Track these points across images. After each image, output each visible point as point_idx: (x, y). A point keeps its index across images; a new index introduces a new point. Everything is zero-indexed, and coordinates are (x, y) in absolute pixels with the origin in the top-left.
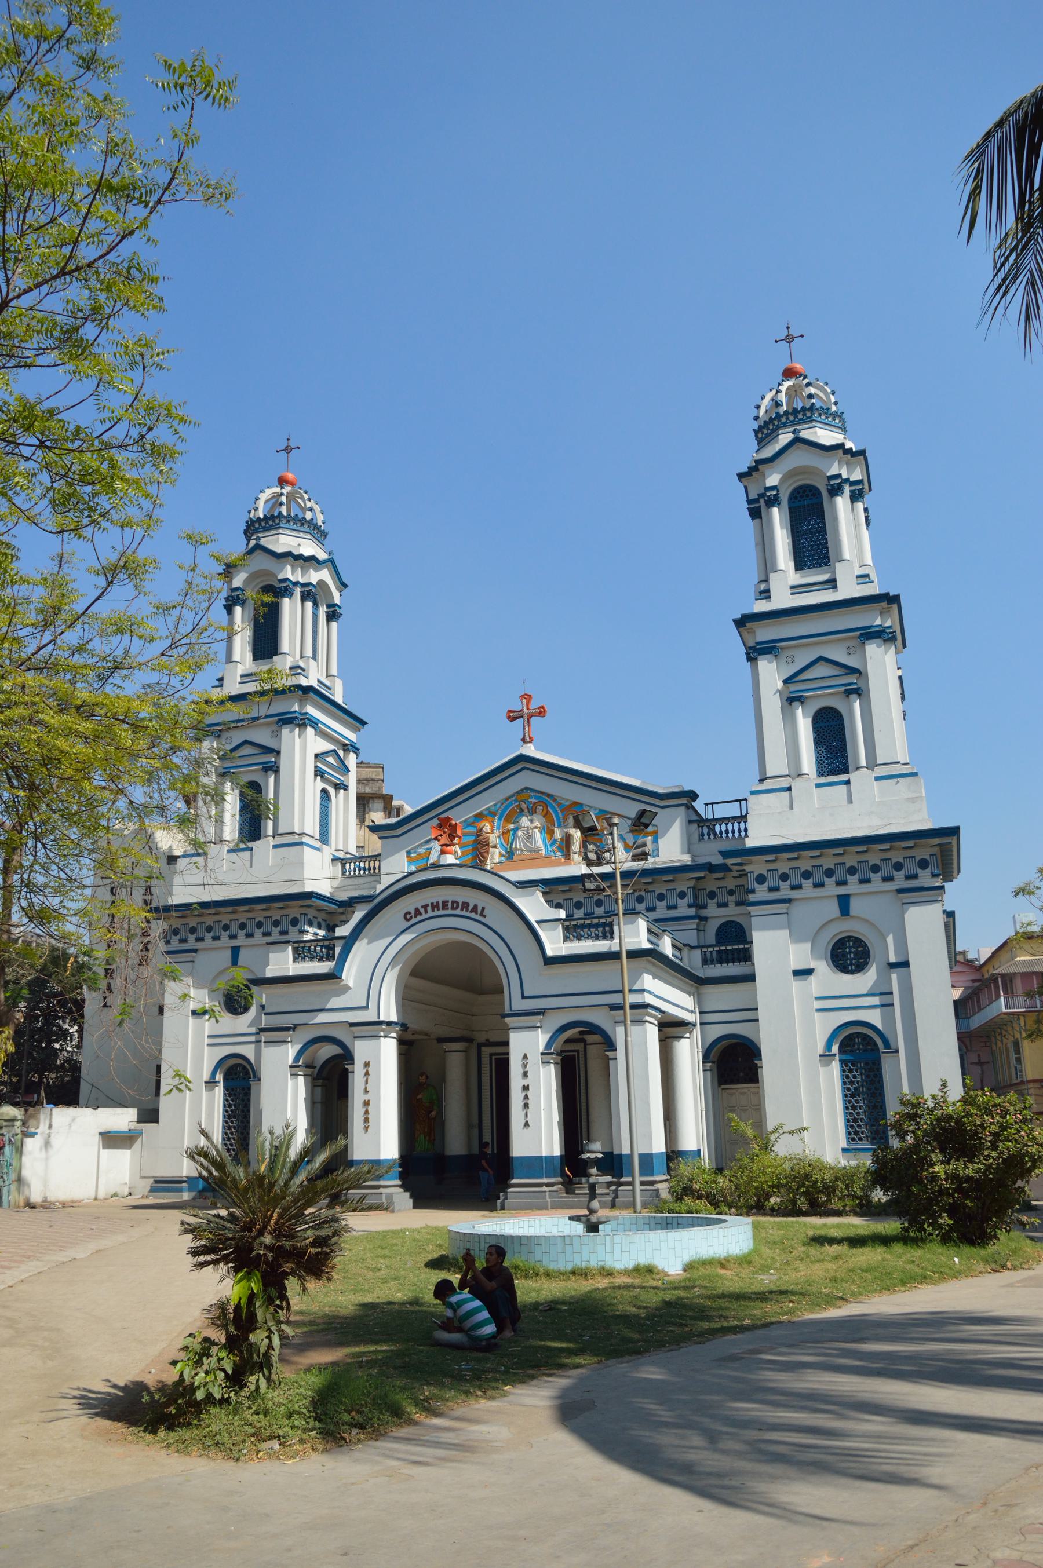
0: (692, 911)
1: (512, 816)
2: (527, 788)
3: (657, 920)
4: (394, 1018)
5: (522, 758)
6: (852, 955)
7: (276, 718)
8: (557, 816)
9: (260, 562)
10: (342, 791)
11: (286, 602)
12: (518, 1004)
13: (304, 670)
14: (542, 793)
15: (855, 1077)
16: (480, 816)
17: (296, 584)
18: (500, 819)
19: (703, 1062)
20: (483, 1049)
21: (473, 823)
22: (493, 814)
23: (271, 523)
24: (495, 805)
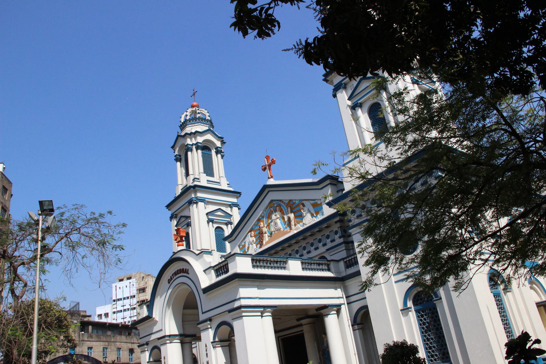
0: (342, 240)
1: (269, 217)
3: (327, 250)
4: (176, 332)
5: (265, 187)
7: (187, 204)
8: (284, 209)
9: (181, 142)
10: (229, 225)
11: (189, 153)
13: (198, 179)
14: (278, 200)
15: (425, 319)
16: (259, 220)
17: (192, 145)
18: (266, 219)
19: (352, 326)
21: (257, 224)
22: (263, 217)
23: (184, 125)
24: (263, 213)
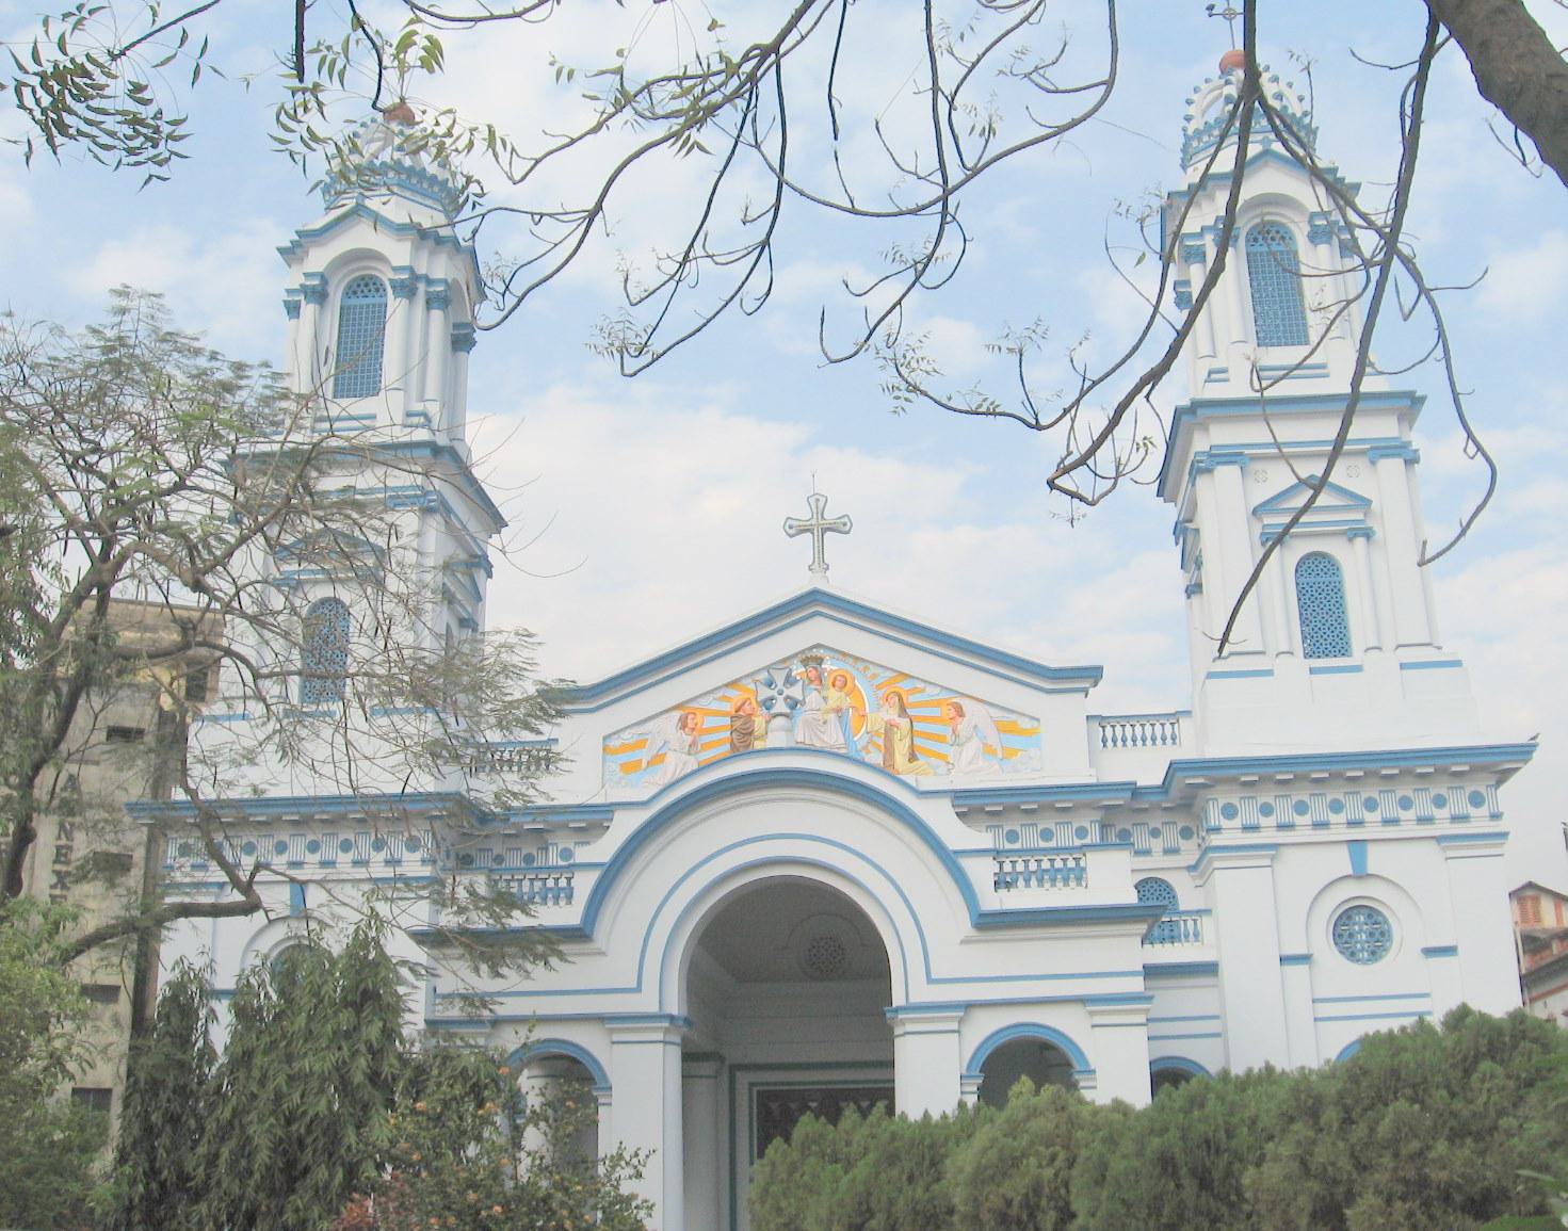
2: (818, 646)
6: (1364, 937)
12: (922, 993)
20: (738, 1074)
